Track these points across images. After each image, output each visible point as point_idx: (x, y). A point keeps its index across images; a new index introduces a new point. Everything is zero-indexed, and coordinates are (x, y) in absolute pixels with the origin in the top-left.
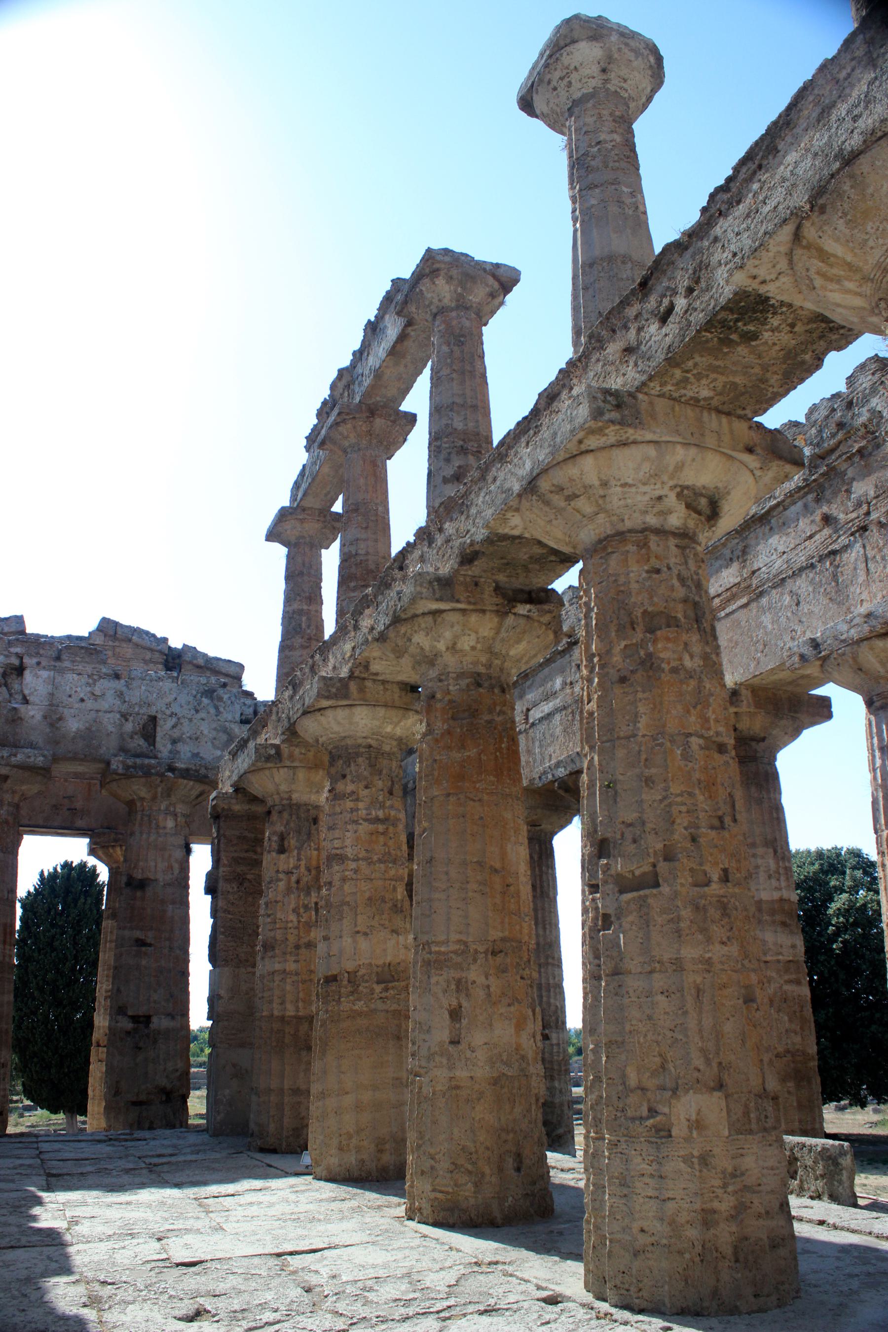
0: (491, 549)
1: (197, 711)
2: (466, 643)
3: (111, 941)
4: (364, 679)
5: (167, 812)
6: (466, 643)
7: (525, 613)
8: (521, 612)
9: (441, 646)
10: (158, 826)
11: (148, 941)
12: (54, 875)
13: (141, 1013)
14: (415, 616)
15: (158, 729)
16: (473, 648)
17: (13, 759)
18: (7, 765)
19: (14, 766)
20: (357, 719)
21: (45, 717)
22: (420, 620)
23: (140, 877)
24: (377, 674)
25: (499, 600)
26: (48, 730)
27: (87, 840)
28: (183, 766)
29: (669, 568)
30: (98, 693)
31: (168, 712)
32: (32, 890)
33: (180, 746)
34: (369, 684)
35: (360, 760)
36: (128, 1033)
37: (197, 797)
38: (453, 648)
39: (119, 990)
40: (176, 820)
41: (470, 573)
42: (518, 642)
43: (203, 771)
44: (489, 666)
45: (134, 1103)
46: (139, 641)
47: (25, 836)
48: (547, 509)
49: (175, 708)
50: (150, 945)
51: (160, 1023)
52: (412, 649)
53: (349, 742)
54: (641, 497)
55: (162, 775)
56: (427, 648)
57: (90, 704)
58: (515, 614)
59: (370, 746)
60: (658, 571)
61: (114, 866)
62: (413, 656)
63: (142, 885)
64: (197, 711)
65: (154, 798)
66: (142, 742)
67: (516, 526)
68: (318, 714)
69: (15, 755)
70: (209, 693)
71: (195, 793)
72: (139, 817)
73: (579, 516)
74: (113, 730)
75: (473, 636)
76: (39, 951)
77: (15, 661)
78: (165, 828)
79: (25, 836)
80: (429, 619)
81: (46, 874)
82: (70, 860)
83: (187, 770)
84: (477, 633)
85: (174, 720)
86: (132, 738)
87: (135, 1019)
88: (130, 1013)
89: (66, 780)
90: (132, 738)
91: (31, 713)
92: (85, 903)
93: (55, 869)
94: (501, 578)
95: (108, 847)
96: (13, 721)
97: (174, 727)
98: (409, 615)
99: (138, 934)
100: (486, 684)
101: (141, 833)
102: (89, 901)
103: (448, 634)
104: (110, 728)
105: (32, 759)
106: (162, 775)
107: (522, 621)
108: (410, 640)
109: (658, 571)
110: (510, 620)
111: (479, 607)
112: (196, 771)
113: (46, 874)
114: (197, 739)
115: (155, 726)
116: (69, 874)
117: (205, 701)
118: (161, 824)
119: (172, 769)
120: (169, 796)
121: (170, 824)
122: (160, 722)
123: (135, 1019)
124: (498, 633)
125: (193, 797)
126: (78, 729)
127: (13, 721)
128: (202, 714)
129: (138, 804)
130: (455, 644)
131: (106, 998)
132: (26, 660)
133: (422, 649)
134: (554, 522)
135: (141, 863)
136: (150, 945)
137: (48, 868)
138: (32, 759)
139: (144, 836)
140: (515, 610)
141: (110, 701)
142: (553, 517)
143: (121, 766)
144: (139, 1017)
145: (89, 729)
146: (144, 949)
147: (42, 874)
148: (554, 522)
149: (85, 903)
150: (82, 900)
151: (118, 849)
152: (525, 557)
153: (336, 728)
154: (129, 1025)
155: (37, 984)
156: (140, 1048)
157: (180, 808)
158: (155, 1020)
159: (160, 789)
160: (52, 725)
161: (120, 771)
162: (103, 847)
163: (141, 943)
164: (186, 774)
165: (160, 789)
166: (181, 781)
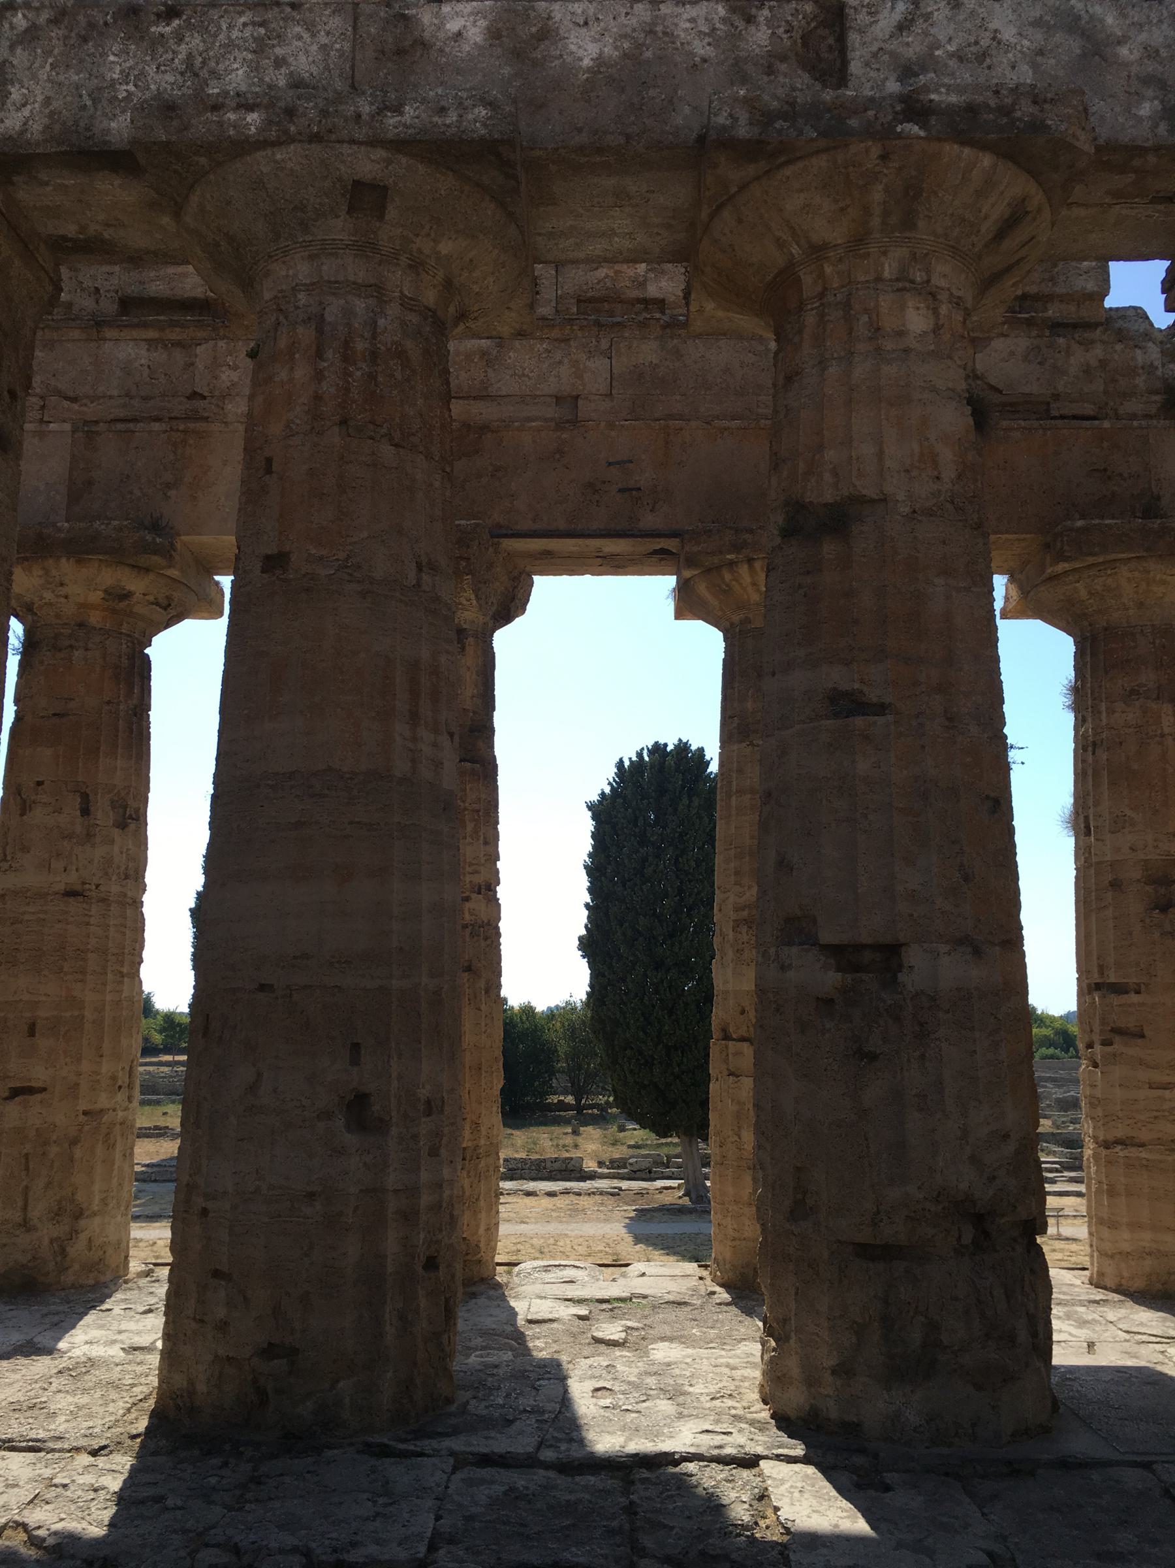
3: (740, 792)
5: (904, 284)
11: (873, 696)
12: (638, 765)
13: (865, 939)
15: (853, 37)
17: (392, 120)
18: (374, 142)
19: (399, 145)
21: (494, 34)
23: (829, 496)
26: (507, 71)
27: (671, 581)
28: (953, 99)
32: (607, 790)
36: (825, 1004)
37: (1000, 235)
39: (784, 865)
40: (935, 311)
43: (1025, 110)
45: (864, 1251)
47: (536, 578)
50: (881, 709)
51: (931, 968)
55: (885, 134)
61: (736, 619)
63: (838, 520)
65: (858, 242)
66: (803, 79)
69: (398, 110)
71: (996, 209)
72: (810, 319)
74: (709, 52)
76: (624, 886)
78: (901, 334)
79: (536, 578)
81: (627, 763)
82: (662, 742)
83: (971, 110)
86: (770, 70)
87: (844, 956)
88: (827, 936)
89: (611, 426)
90: (770, 70)
91: (453, 26)
92: (689, 806)
93: (640, 755)
95: (718, 568)
96: (400, 52)
97: (903, 27)
99: (837, 677)
101: (822, 364)
102: (696, 802)
104: (701, 48)
105: (452, 117)
106: (885, 134)
112: (1005, 111)
113: (627, 763)
114: (983, 56)
115: (841, 39)
116: (662, 763)
119: (914, 108)
120: (908, 223)
121: (917, 320)
123: (844, 956)
125: (988, 228)
126: (599, 60)
127: (400, 52)
129: (807, 279)
131: (737, 924)
135: (830, 455)
136: (881, 709)
137: (629, 755)
138: (452, 117)
139: (833, 370)
143: (743, 116)
144: (860, 947)
145: (632, 57)
146: (859, 722)
147: (620, 764)
149: (689, 806)
150: (685, 801)
151: (744, 570)
154: (830, 979)
155: (624, 934)
156: (872, 1057)
157: (946, 274)
158: (914, 957)
159: (877, 195)
160: (518, 54)
161: (743, 131)
162: (709, 570)
163: (847, 704)
164: (966, 124)
165: (877, 195)
166: (950, 149)
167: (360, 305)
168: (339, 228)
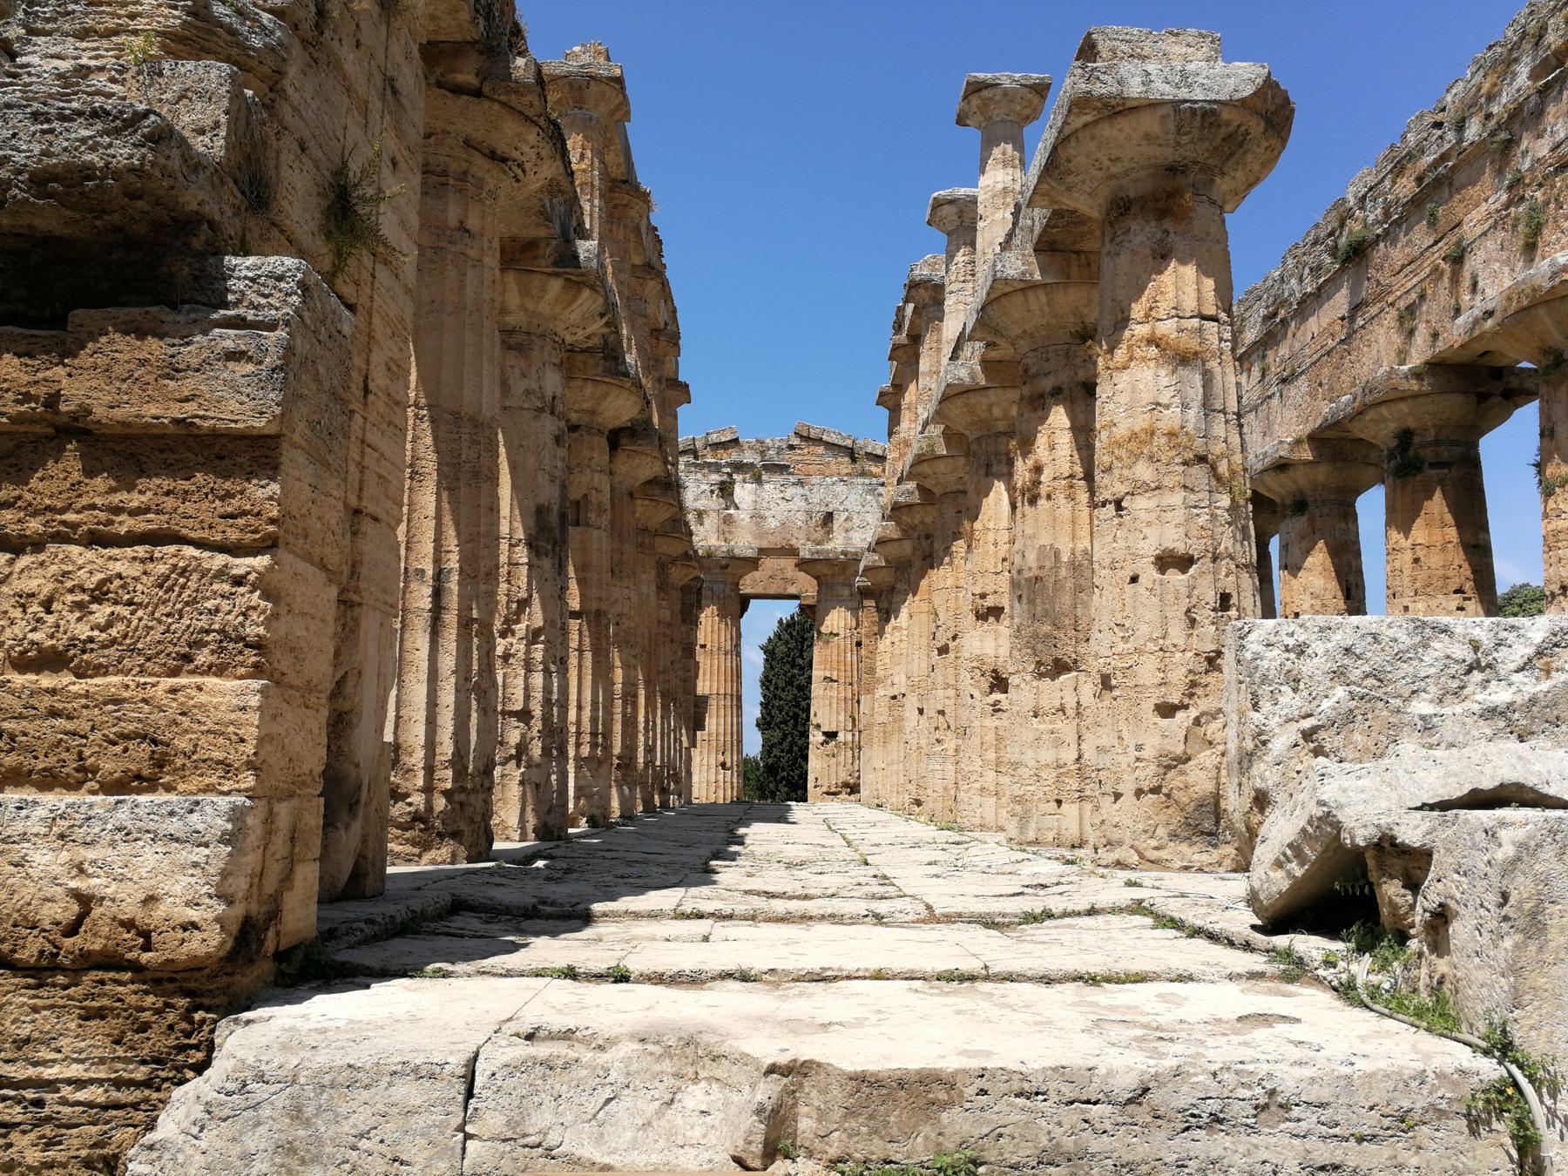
6: (928, 520)
38: (922, 522)
54: (953, 478)
70: (872, 491)
77: (725, 478)
122: (836, 516)
128: (868, 508)
141: (799, 503)
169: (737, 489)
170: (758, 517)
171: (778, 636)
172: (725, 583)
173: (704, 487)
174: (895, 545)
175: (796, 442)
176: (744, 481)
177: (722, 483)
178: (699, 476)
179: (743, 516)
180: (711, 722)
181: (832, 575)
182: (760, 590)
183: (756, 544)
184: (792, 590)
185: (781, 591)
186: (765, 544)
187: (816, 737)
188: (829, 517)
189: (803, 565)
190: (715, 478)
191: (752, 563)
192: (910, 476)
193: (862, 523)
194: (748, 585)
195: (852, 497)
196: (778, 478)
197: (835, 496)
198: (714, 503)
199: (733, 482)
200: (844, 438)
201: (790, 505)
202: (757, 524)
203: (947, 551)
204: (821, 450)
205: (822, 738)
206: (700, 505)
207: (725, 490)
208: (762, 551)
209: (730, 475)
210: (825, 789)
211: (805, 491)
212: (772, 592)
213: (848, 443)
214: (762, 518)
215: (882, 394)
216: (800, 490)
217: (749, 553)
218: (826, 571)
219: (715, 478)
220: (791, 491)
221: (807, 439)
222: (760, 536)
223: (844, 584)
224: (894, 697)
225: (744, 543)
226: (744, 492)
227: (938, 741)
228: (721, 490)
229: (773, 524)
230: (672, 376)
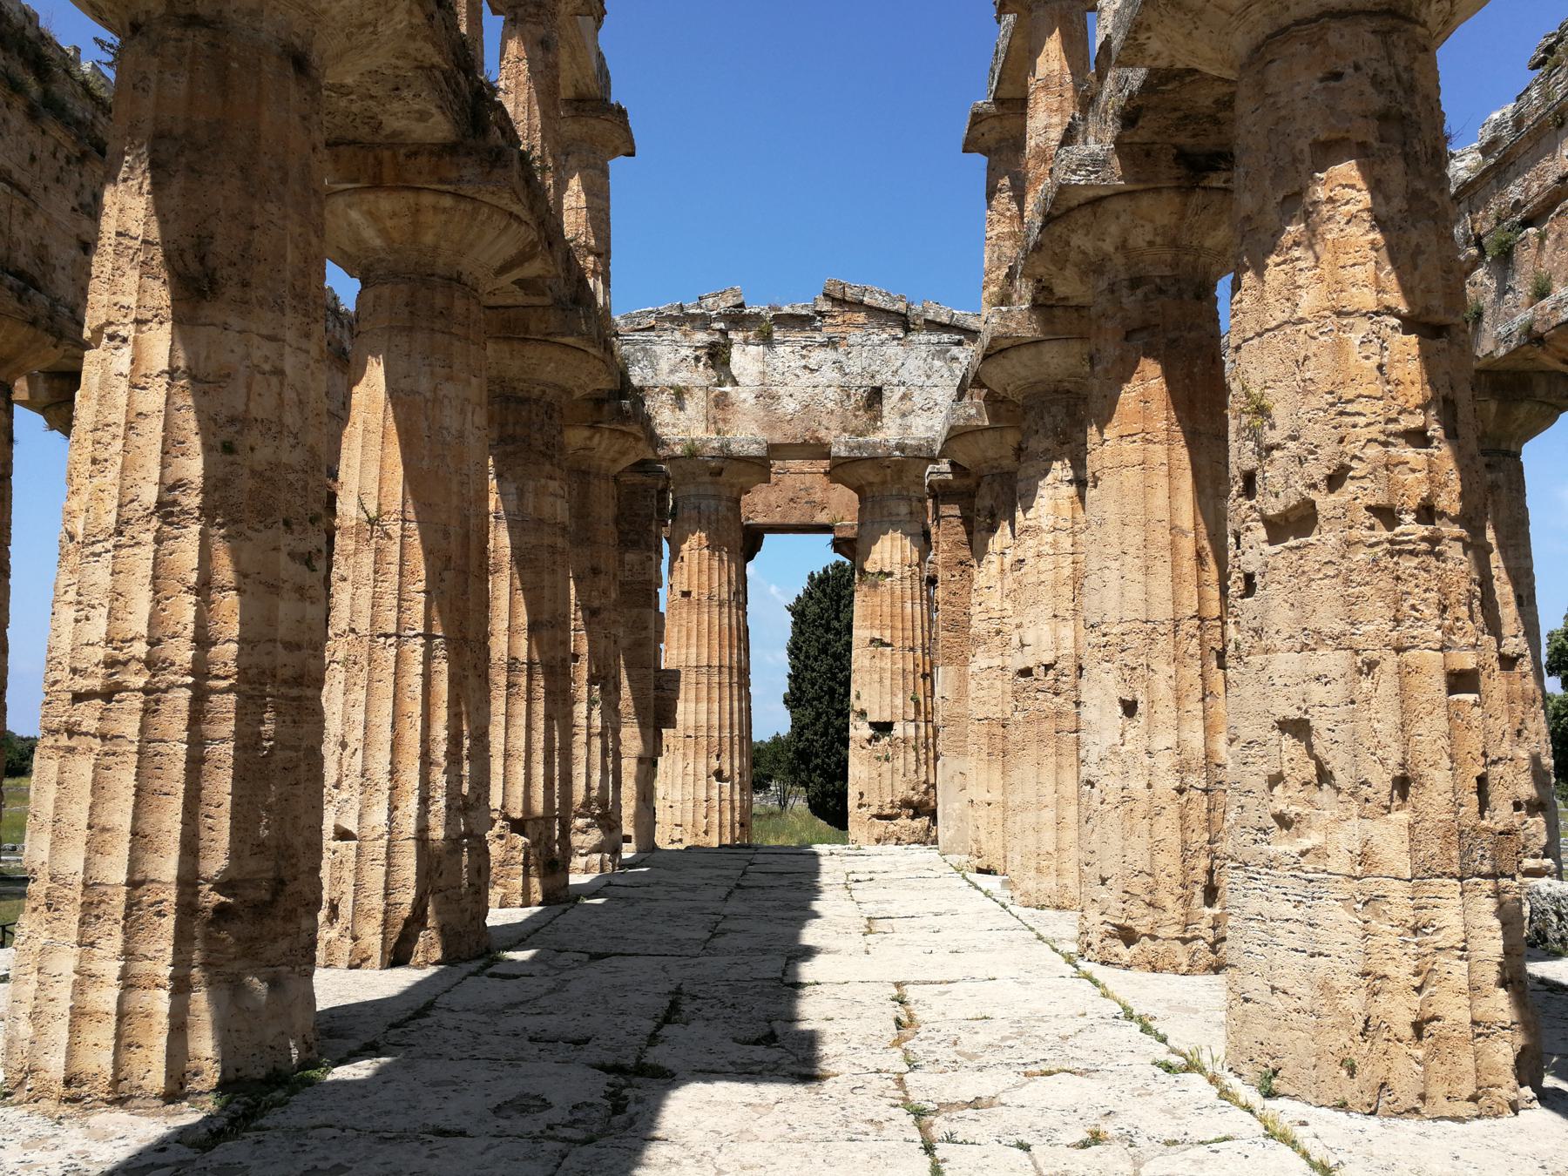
0: (1155, 99)
1: (928, 377)
2: (1139, 239)
4: (1052, 306)
7: (1221, 184)
8: (1214, 184)
9: (1108, 246)
10: (890, 514)
14: (1070, 210)
16: (1151, 243)
20: (1047, 358)
22: (1076, 214)
24: (1066, 298)
25: (1183, 172)
29: (1357, 68)
30: (813, 364)
31: (895, 381)
33: (910, 419)
34: (1058, 312)
35: (1054, 409)
38: (1123, 246)
41: (1137, 139)
42: (1215, 227)
44: (1175, 264)
46: (873, 303)
48: (1180, 15)
49: (904, 374)
52: (1073, 256)
53: (1040, 388)
56: (1091, 252)
57: (806, 377)
58: (1204, 188)
59: (1068, 391)
60: (1337, 76)
62: (1076, 265)
64: (928, 377)
67: (1159, 54)
68: (1000, 357)
73: (1225, 17)
75: (1149, 227)
80: (1088, 211)
84: (1151, 221)
85: (903, 389)
91: (743, 396)
93: (825, 571)
94: (1183, 139)
98: (1063, 209)
100: (1173, 290)
103: (1114, 229)
107: (1217, 197)
108: (1068, 244)
109: (1337, 76)
110: (1197, 198)
111: (1152, 185)
117: (937, 363)
118: (894, 511)
120: (900, 478)
122: (887, 393)
124: (1182, 218)
128: (935, 379)
130: (1125, 241)
132: (732, 335)
133: (1084, 253)
134: (1196, 33)
140: (1205, 183)
141: (829, 374)
142: (1191, 26)
147: (811, 576)
148: (1196, 33)
152: (1209, 102)
153: (1023, 372)
167: (713, 502)
168: (707, 478)
169: (736, 355)
170: (767, 396)
171: (808, 594)
172: (717, 497)
173: (684, 352)
174: (1026, 354)
175: (825, 306)
176: (746, 342)
177: (713, 345)
178: (678, 335)
179: (744, 395)
180: (688, 710)
181: (884, 487)
182: (776, 518)
183: (763, 436)
184: (822, 518)
185: (806, 520)
186: (778, 438)
187: (859, 731)
188: (875, 396)
189: (841, 470)
190: (702, 337)
191: (759, 467)
192: (978, 382)
193: (925, 401)
194: (759, 505)
195: (912, 364)
196: (797, 336)
197: (886, 362)
198: (700, 376)
199: (729, 344)
200: (893, 301)
201: (817, 378)
202: (767, 407)
203: (1295, 203)
204: (861, 317)
205: (868, 732)
206: (678, 379)
207: (717, 356)
208: (775, 450)
209: (724, 333)
210: (874, 810)
211: (839, 355)
212: (793, 521)
213: (900, 306)
214: (774, 397)
215: (977, 118)
216: (830, 355)
217: (754, 450)
218: (872, 476)
219: (702, 337)
220: (817, 356)
221: (841, 302)
222: (771, 427)
223: (900, 497)
224: (1026, 672)
225: (746, 434)
226: (745, 359)
227: (1283, 821)
228: (711, 356)
229: (789, 406)
230: (594, 90)
